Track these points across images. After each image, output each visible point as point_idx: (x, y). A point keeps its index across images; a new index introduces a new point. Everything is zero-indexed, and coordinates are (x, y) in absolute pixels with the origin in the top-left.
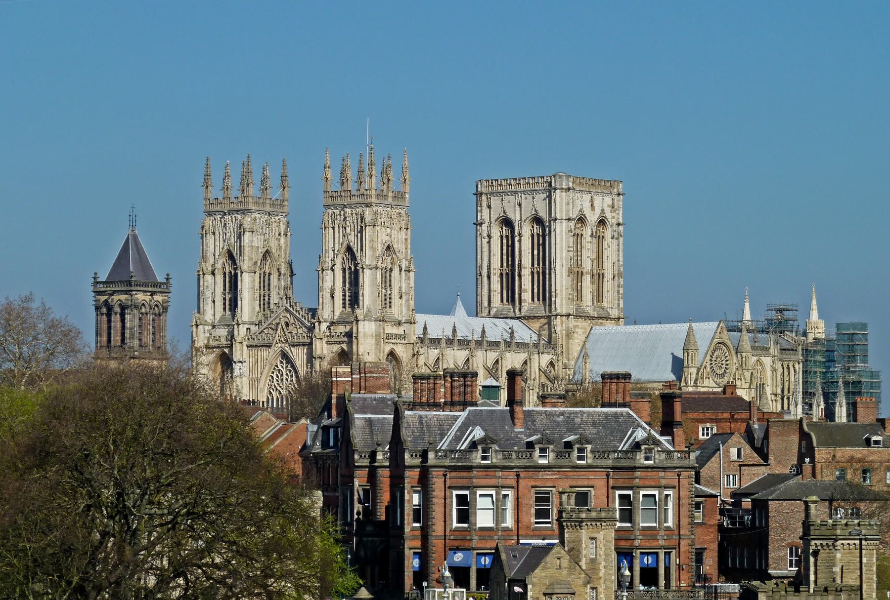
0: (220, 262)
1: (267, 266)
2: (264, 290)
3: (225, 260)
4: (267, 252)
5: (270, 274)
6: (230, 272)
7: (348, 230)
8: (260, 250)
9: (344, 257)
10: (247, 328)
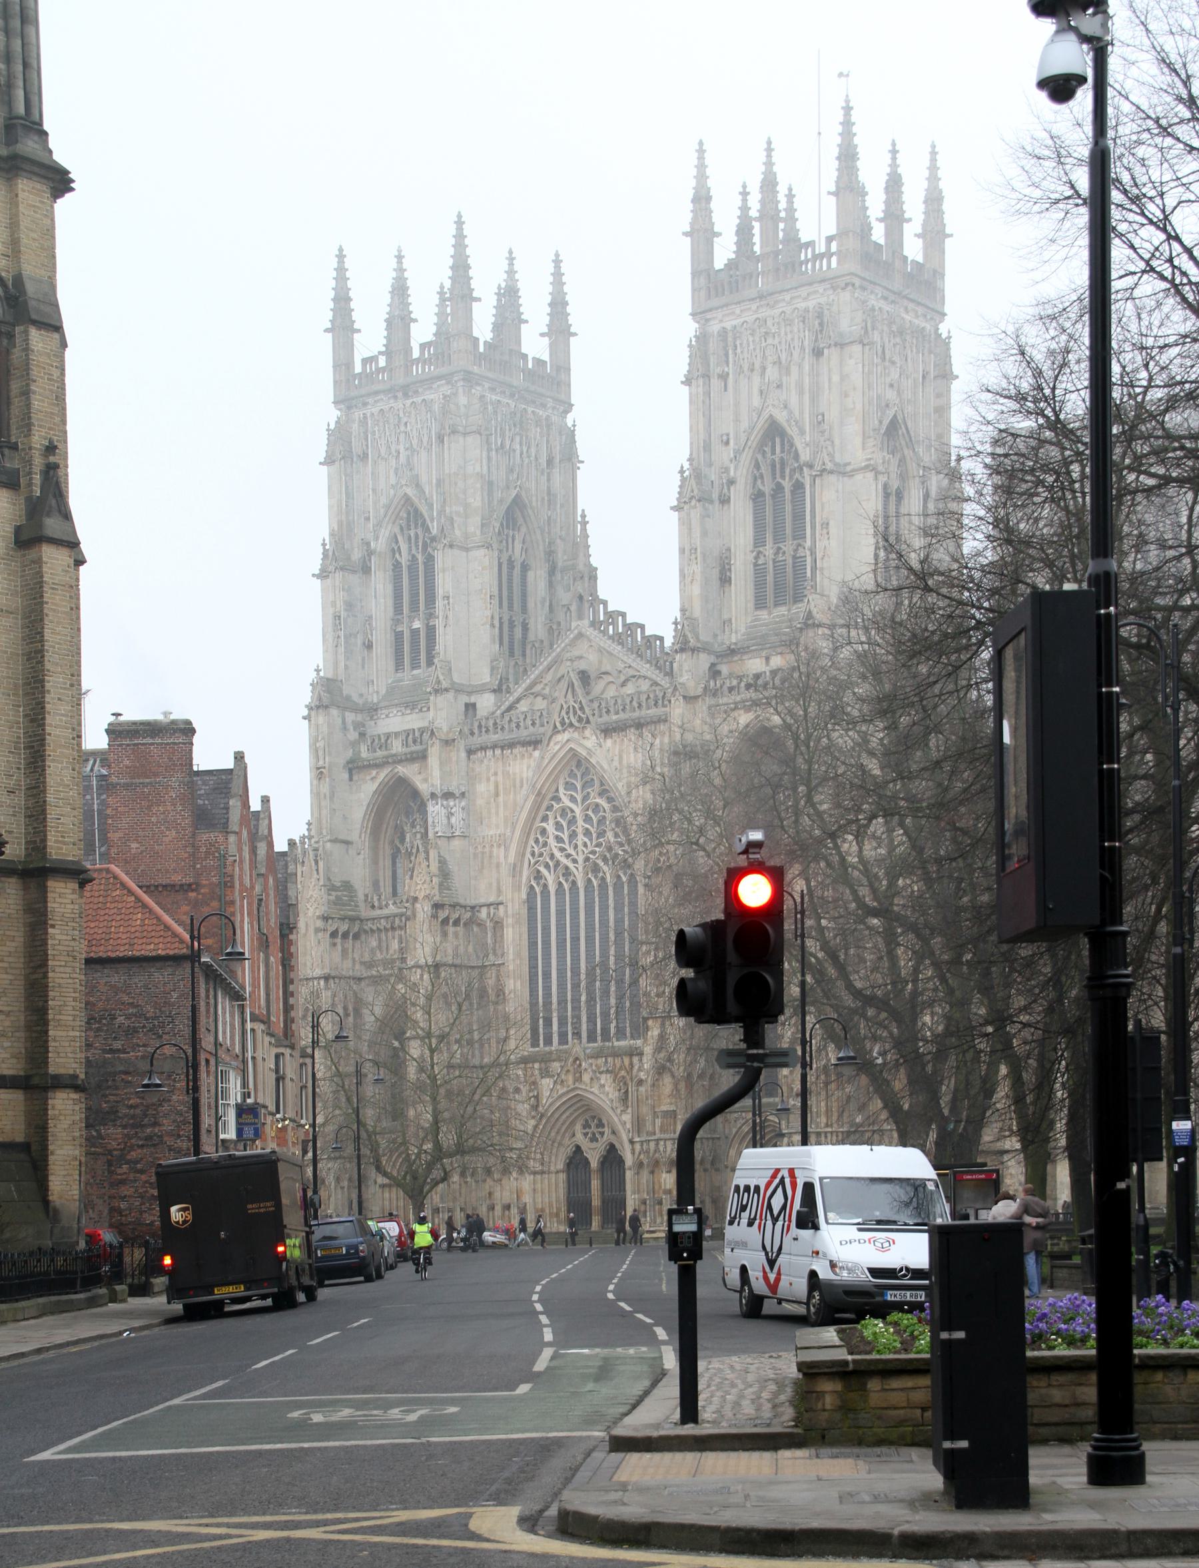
0: (385, 533)
1: (518, 546)
2: (511, 607)
3: (397, 530)
4: (517, 502)
5: (525, 568)
6: (414, 558)
7: (772, 373)
8: (498, 495)
9: (760, 457)
10: (467, 705)
